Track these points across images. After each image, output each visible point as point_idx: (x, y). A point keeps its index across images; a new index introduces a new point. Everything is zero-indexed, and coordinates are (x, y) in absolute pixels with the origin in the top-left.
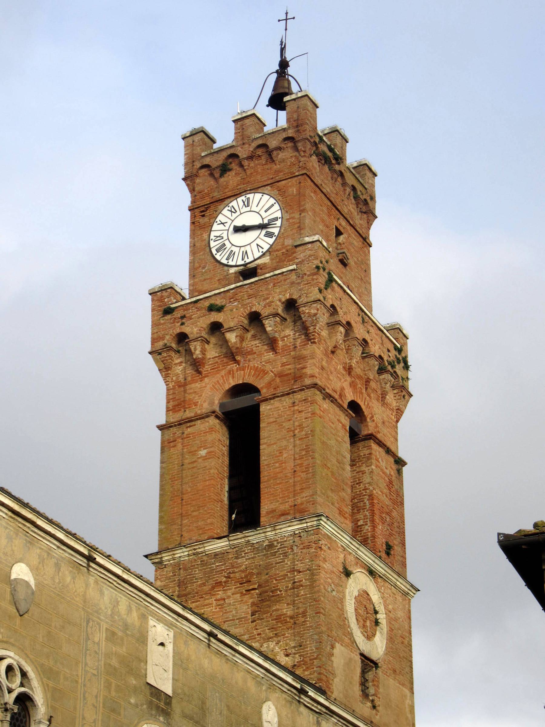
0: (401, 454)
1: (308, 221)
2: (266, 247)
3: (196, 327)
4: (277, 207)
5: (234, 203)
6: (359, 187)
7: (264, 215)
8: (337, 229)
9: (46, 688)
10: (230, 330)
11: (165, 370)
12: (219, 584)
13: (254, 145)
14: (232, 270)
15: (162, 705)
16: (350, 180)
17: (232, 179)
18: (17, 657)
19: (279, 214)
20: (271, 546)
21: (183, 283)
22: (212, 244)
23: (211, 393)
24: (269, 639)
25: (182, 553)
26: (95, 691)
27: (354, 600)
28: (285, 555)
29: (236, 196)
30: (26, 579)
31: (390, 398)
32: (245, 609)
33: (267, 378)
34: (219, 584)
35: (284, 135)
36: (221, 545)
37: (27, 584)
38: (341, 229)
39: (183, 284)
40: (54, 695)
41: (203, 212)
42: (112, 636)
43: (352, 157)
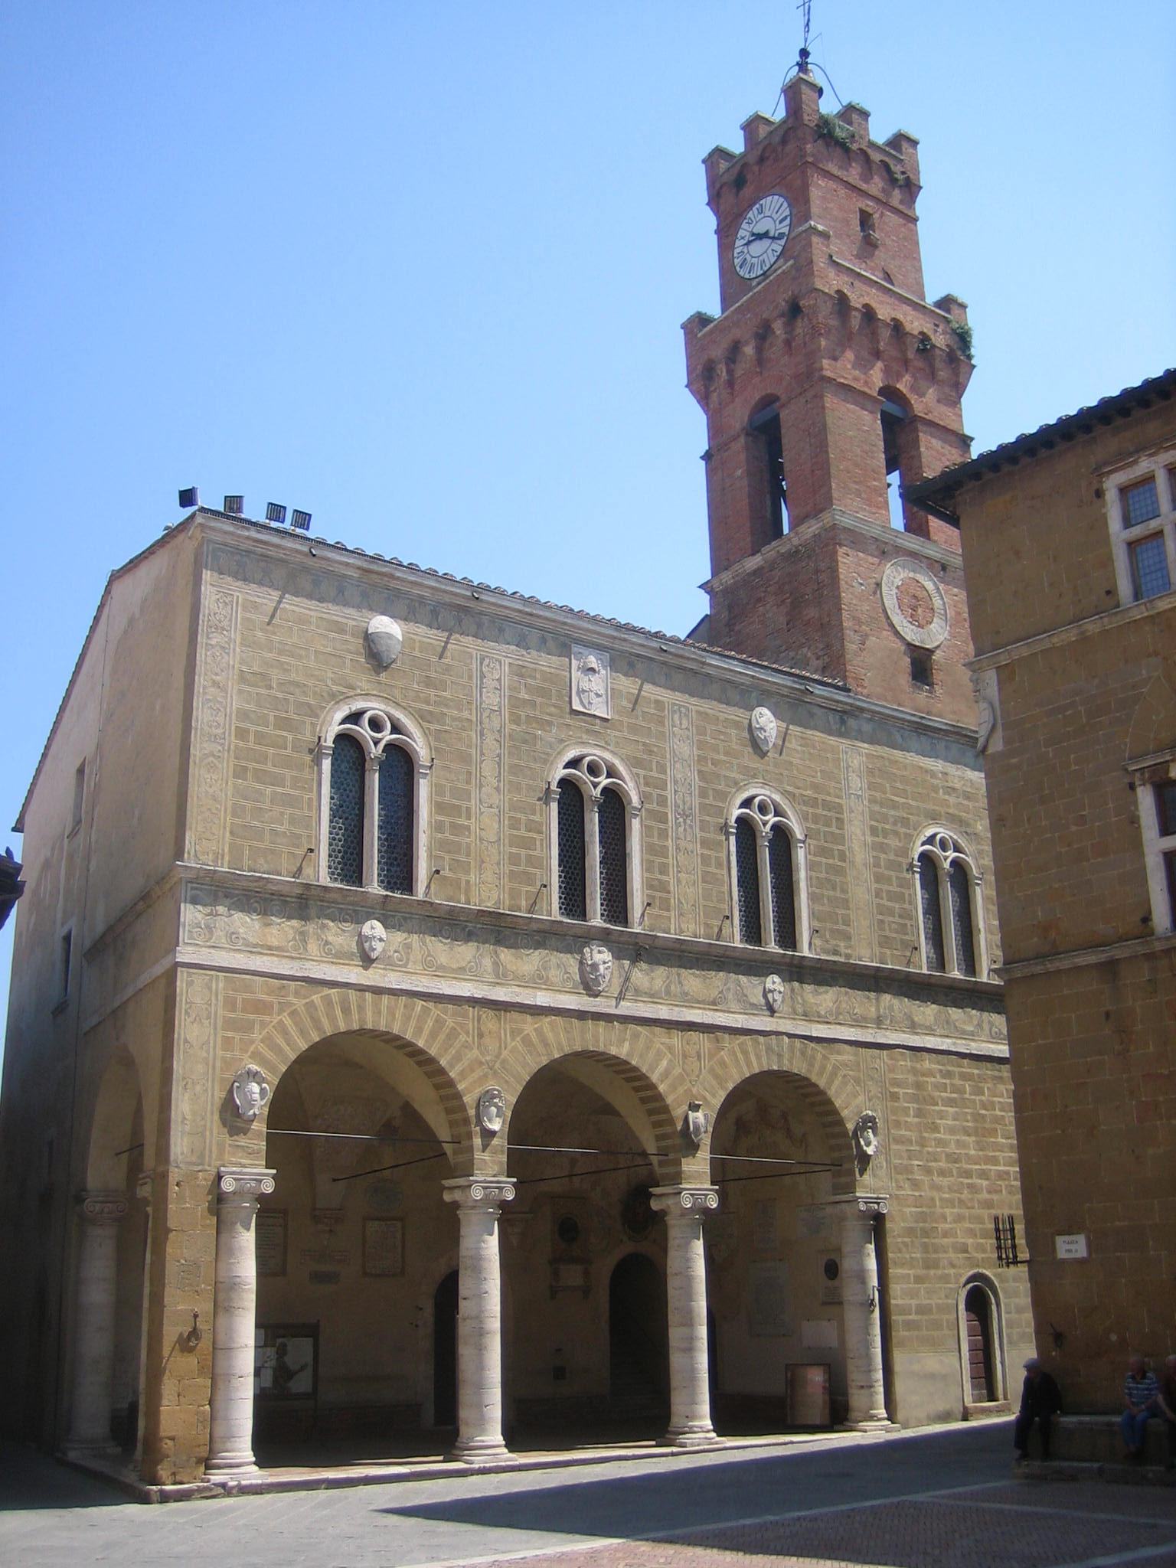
0: (967, 431)
1: (815, 210)
2: (779, 249)
3: (718, 352)
4: (785, 205)
5: (750, 215)
6: (891, 163)
7: (775, 216)
8: (862, 211)
9: (426, 733)
10: (747, 343)
11: (704, 399)
12: (759, 600)
13: (761, 147)
14: (754, 283)
15: (596, 728)
16: (876, 157)
17: (747, 191)
18: (383, 707)
19: (787, 212)
20: (797, 552)
21: (713, 309)
22: (736, 261)
23: (739, 415)
24: (802, 646)
25: (727, 577)
26: (496, 725)
27: (895, 591)
28: (809, 557)
29: (750, 207)
30: (387, 630)
31: (943, 374)
32: (782, 620)
33: (785, 383)
34: (759, 600)
35: (785, 127)
36: (753, 562)
37: (390, 636)
38: (869, 210)
39: (713, 309)
40: (434, 737)
41: (726, 234)
42: (519, 672)
43: (879, 132)
